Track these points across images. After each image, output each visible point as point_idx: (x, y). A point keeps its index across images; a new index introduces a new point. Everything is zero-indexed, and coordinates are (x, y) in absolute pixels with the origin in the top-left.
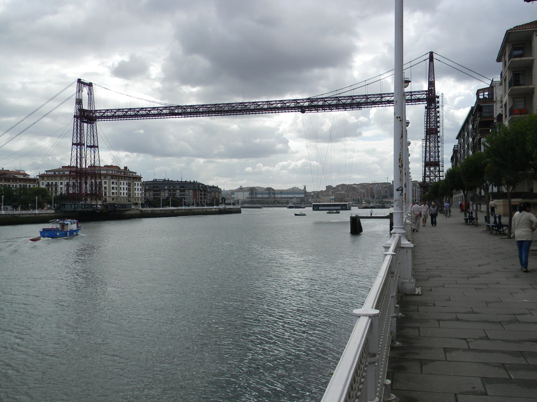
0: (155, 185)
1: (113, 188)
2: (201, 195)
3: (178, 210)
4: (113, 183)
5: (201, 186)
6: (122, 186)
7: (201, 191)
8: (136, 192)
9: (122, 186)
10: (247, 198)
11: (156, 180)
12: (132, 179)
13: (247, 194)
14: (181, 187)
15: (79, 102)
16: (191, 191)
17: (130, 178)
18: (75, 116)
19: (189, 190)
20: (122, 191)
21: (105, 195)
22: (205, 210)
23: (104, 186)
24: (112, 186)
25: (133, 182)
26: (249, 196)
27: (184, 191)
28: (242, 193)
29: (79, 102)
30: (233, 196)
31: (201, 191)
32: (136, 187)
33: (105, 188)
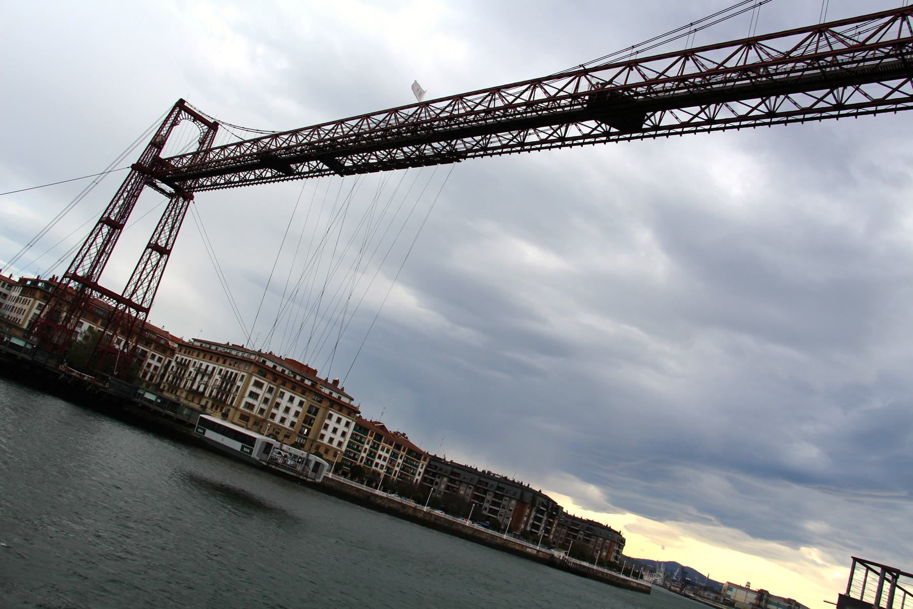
0: (456, 470)
1: (253, 395)
2: (536, 518)
3: (404, 506)
4: (258, 385)
5: (539, 499)
6: (284, 403)
7: (539, 511)
8: (328, 434)
9: (284, 403)
10: (750, 603)
11: (489, 473)
12: (326, 404)
13: (752, 598)
14: (499, 488)
15: (158, 143)
16: (514, 502)
17: (322, 397)
18: (134, 167)
19: (511, 498)
20: (280, 413)
21: (232, 403)
22: (498, 541)
23: (239, 383)
24: (251, 388)
25: (327, 409)
26: (754, 601)
27: (501, 497)
28: (744, 593)
29: (158, 143)
30: (729, 593)
31: (542, 512)
32: (332, 424)
33: (238, 387)
